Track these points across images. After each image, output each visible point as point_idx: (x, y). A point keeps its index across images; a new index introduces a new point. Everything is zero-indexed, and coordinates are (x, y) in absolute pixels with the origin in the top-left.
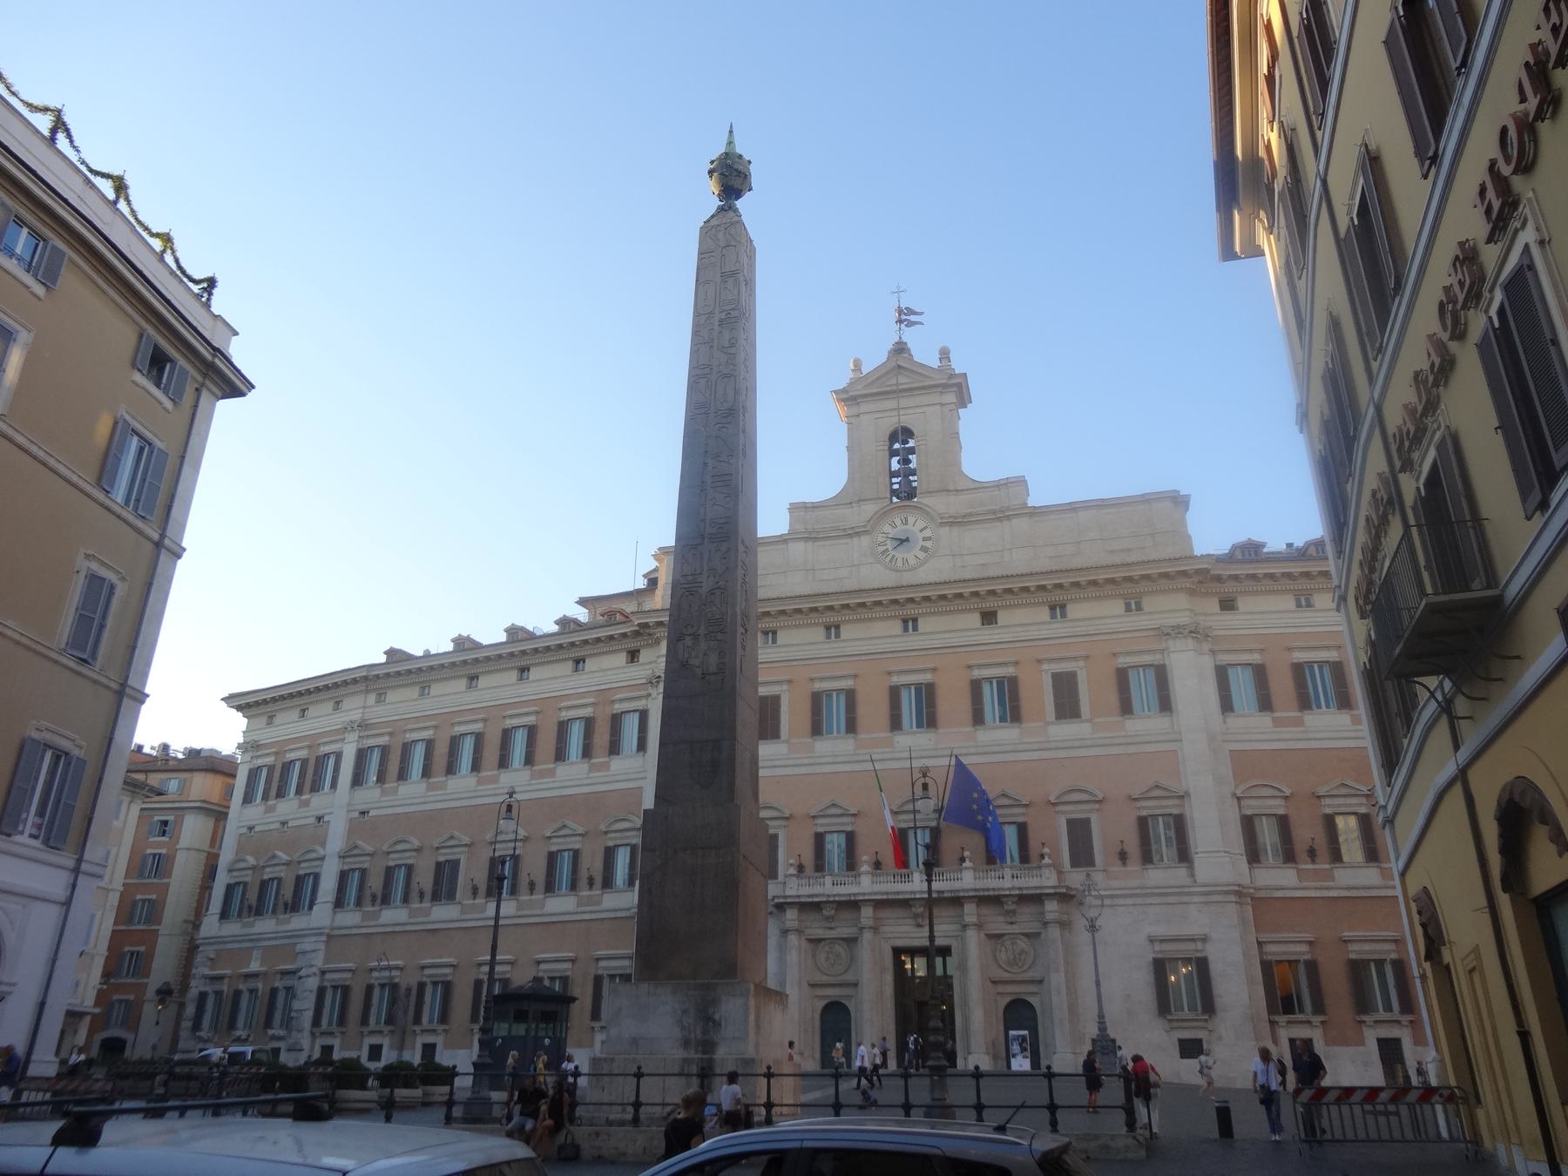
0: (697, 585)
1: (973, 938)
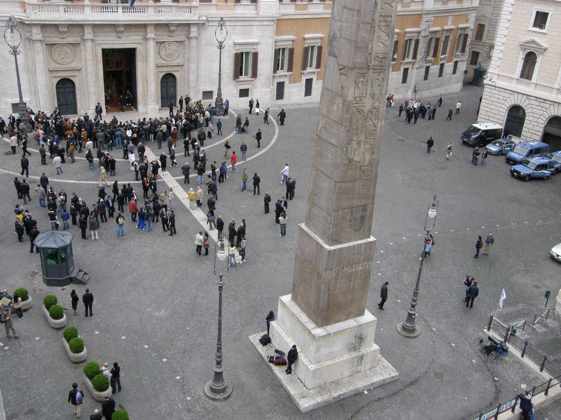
1: (151, 45)
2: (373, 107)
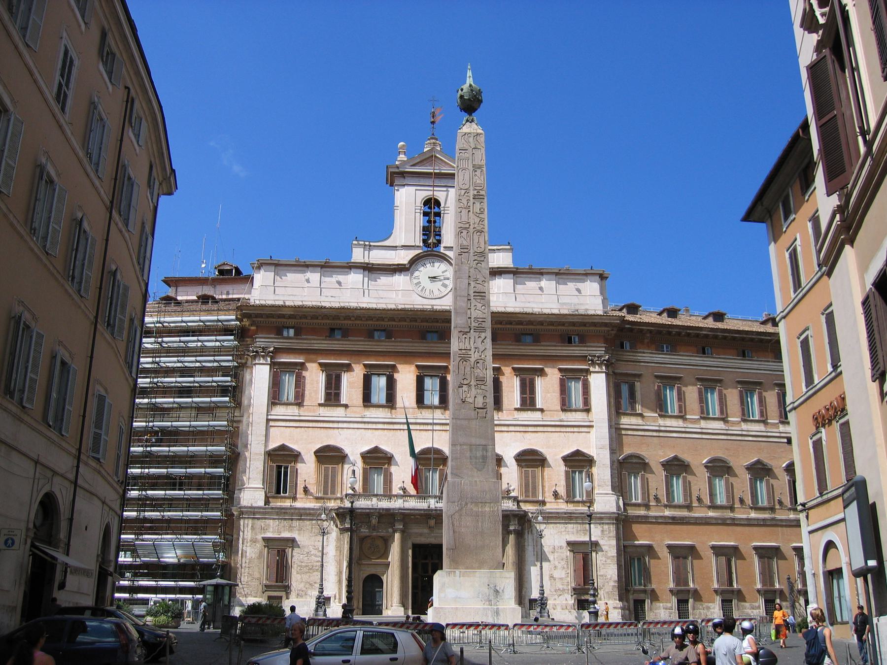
0: (469, 356)
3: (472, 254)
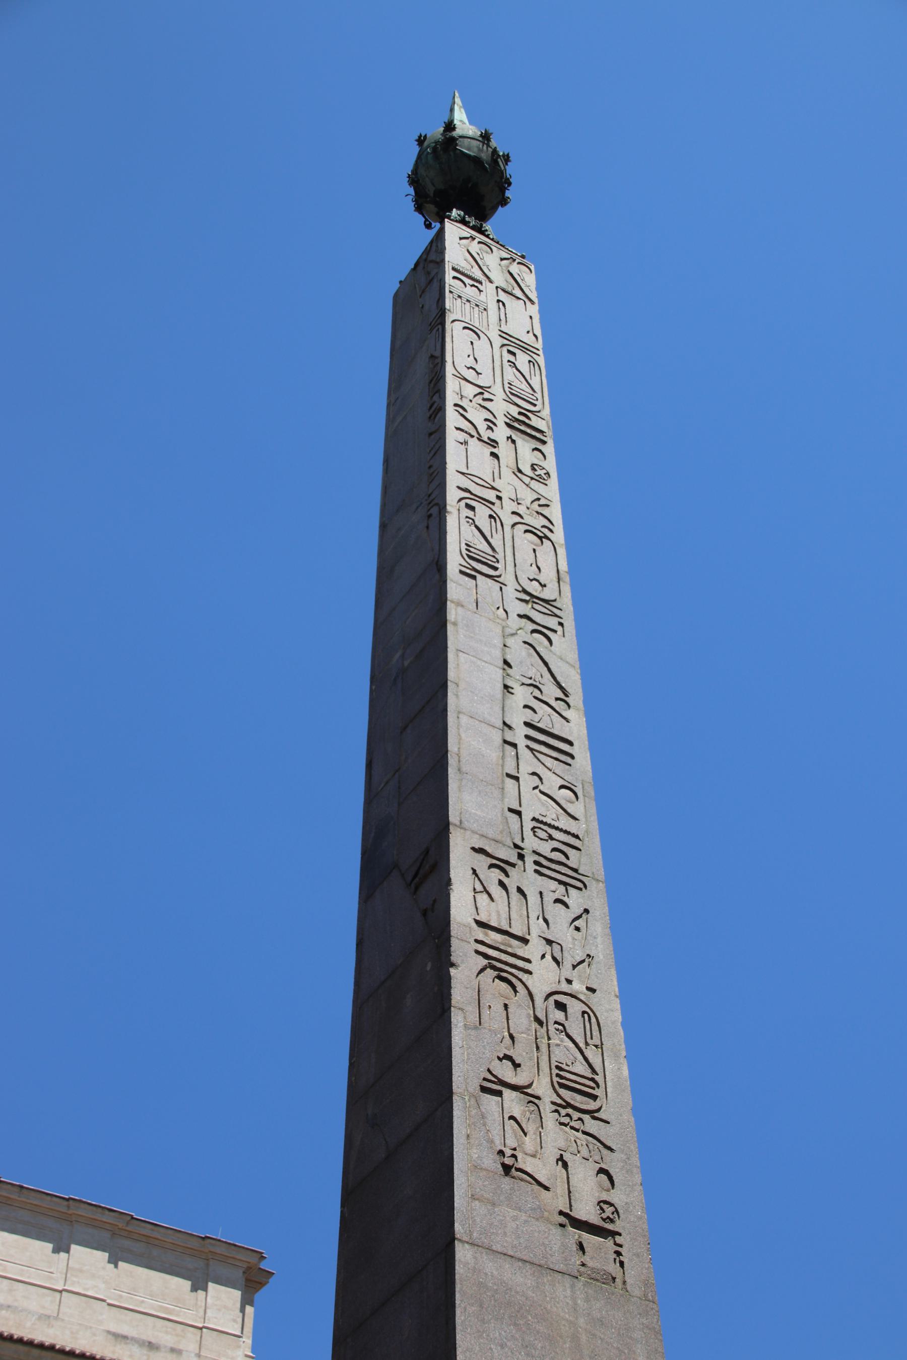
0: (520, 963)
2: (564, 987)
3: (511, 591)
